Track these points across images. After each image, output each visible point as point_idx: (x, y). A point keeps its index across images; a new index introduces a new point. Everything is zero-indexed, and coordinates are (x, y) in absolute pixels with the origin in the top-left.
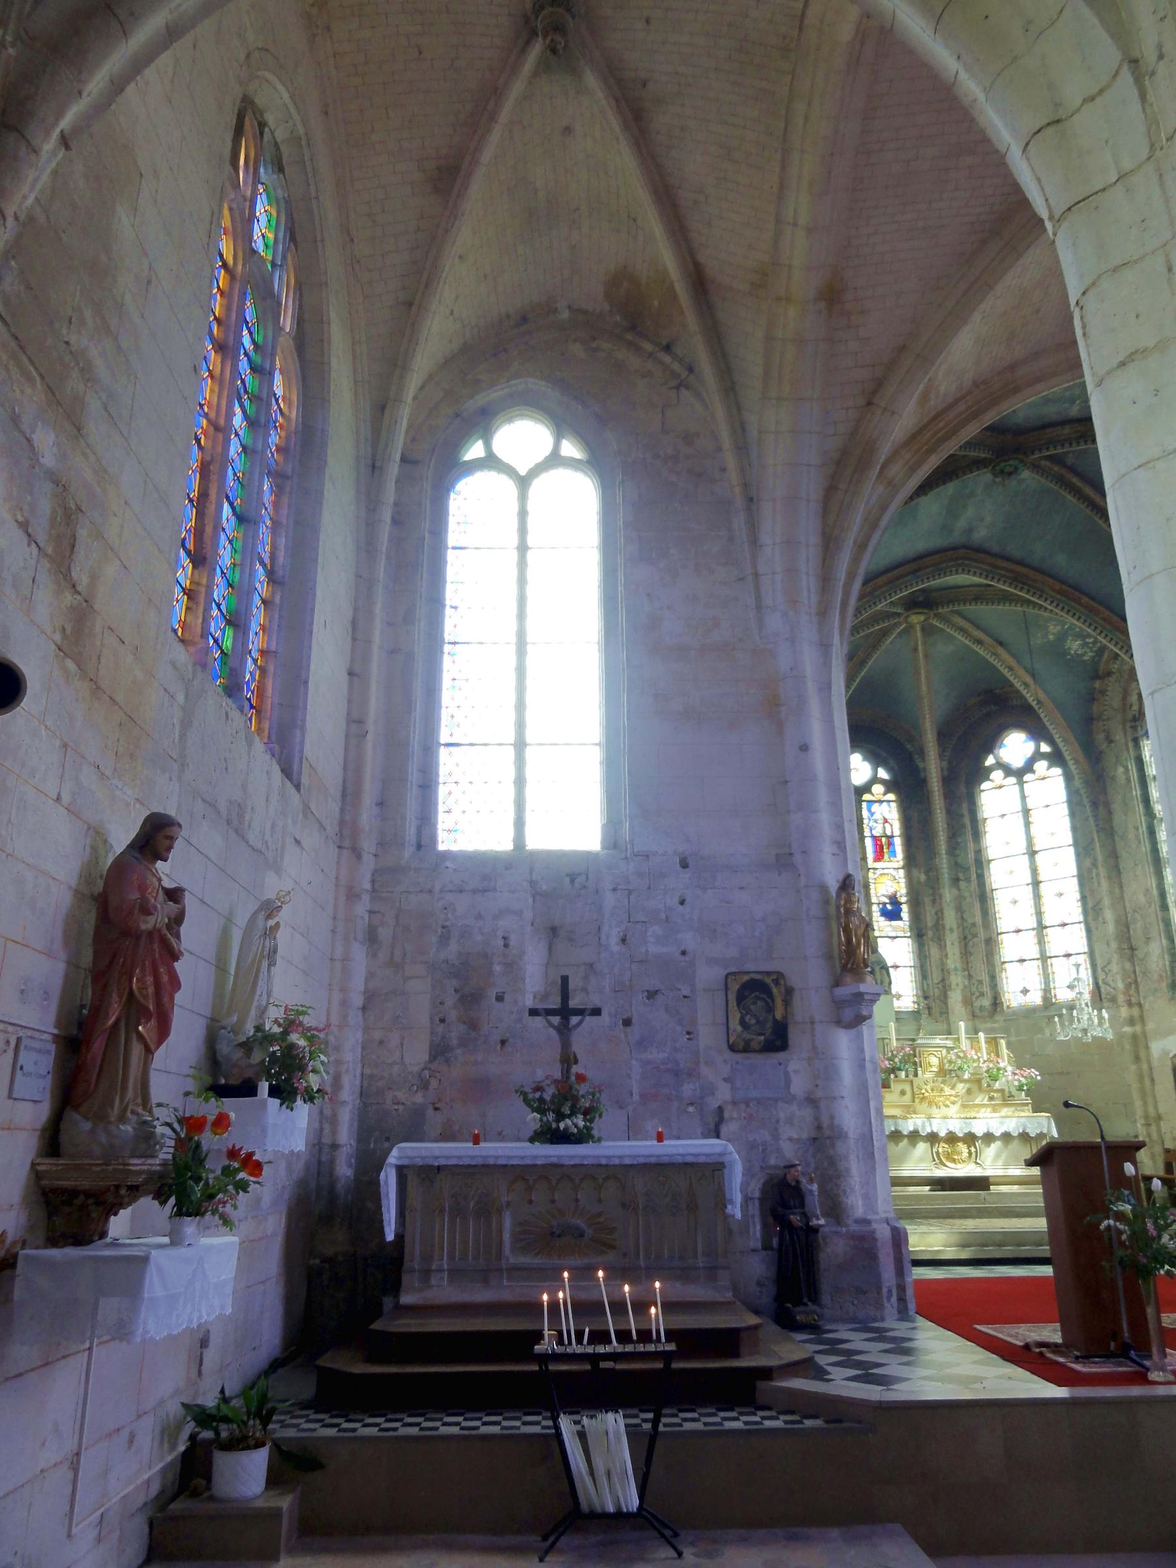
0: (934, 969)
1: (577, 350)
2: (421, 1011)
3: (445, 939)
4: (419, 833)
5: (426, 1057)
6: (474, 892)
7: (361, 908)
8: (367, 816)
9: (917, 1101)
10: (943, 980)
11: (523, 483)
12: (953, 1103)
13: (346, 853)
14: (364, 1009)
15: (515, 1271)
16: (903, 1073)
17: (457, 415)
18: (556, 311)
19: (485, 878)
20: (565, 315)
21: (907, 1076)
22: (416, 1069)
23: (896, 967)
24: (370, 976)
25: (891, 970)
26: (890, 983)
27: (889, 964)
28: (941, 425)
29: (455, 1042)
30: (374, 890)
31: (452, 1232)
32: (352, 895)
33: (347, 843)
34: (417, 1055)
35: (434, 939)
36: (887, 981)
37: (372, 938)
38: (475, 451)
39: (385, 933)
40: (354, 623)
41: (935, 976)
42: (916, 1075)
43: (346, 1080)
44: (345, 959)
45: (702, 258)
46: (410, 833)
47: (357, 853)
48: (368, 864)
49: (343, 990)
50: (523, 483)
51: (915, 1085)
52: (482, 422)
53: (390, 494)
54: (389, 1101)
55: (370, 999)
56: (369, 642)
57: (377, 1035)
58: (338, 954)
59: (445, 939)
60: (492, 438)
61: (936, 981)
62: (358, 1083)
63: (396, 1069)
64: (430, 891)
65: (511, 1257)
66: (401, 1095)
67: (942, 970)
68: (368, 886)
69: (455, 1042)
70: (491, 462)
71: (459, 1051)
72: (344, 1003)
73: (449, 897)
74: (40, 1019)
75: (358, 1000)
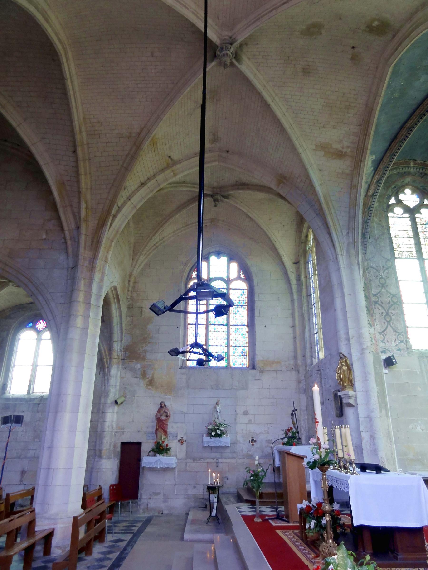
13: (297, 372)
28: (360, 149)
32: (299, 382)
62: (307, 429)
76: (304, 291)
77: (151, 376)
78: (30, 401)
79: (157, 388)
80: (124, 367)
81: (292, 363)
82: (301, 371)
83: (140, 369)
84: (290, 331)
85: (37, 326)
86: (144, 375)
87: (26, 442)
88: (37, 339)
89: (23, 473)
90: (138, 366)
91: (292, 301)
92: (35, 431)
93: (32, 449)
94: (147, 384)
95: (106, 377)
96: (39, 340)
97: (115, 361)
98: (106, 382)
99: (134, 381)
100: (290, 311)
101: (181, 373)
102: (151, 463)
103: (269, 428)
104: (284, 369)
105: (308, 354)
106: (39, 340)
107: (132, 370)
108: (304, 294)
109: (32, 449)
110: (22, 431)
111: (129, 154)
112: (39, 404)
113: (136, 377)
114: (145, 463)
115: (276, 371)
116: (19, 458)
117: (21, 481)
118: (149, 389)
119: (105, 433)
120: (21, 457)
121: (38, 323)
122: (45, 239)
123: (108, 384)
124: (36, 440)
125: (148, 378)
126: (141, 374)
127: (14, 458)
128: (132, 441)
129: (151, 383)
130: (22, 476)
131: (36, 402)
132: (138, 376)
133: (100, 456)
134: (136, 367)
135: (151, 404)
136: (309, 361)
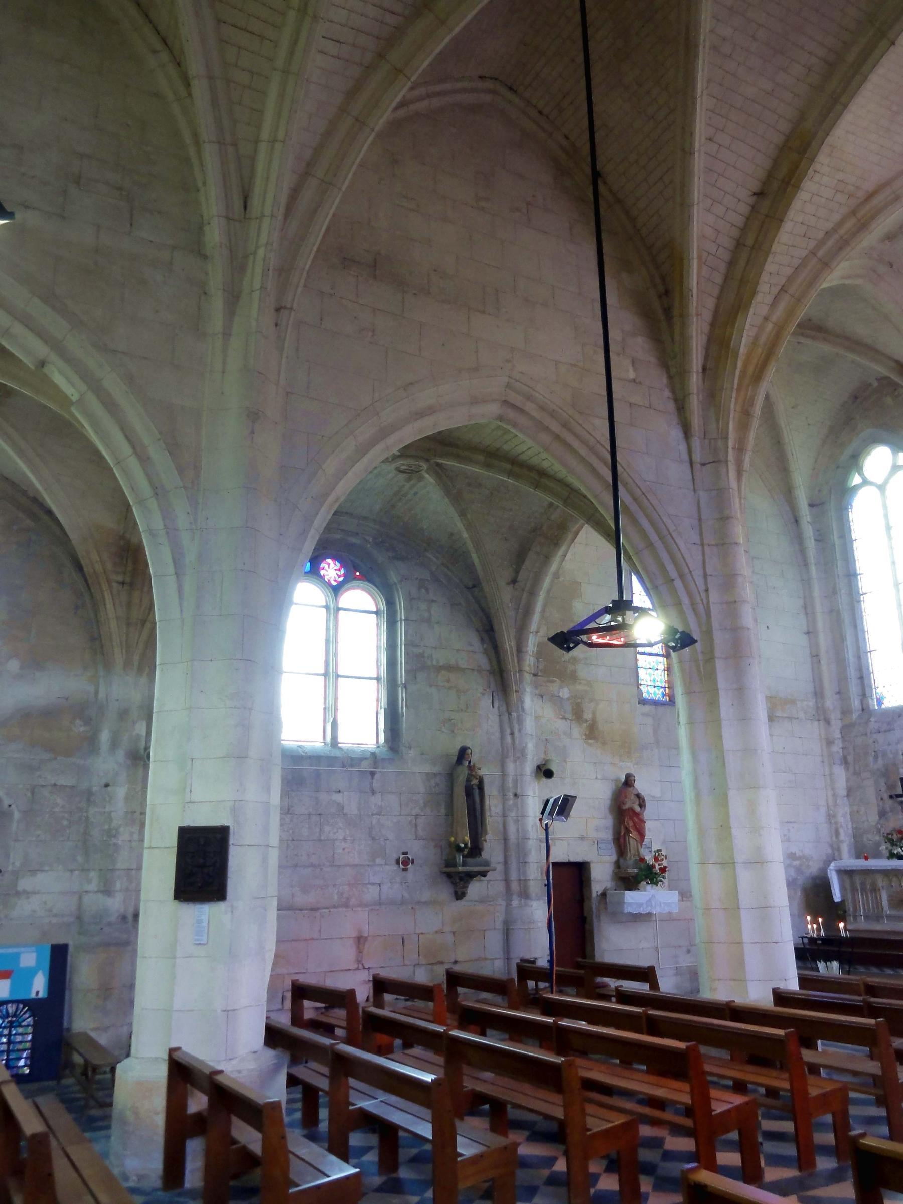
1: (889, 401)
2: (870, 793)
3: (876, 757)
4: (862, 704)
5: (877, 817)
6: (885, 732)
7: (837, 748)
8: (830, 701)
11: (882, 488)
13: (822, 723)
14: (848, 796)
15: (889, 917)
17: (838, 467)
18: (870, 385)
19: (889, 724)
20: (876, 384)
22: (874, 824)
24: (848, 780)
29: (888, 809)
30: (842, 737)
31: (863, 898)
32: (830, 743)
33: (822, 718)
34: (873, 818)
35: (871, 759)
37: (845, 761)
38: (856, 479)
39: (850, 758)
40: (805, 607)
43: (841, 831)
44: (831, 774)
45: (896, 357)
46: (856, 704)
47: (828, 722)
48: (836, 726)
49: (833, 789)
50: (882, 488)
52: (854, 462)
53: (809, 532)
54: (865, 839)
55: (850, 792)
56: (814, 613)
57: (855, 808)
58: (827, 773)
59: (876, 757)
60: (862, 468)
62: (850, 831)
63: (866, 823)
64: (866, 735)
65: (887, 910)
66: (870, 836)
68: (839, 736)
69: (888, 809)
70: (865, 482)
71: (890, 814)
72: (834, 795)
73: (875, 736)
74: (608, 835)
75: (842, 792)
76: (840, 564)
77: (590, 716)
78: (352, 765)
79: (604, 744)
80: (537, 692)
81: (811, 703)
82: (833, 722)
83: (568, 699)
84: (803, 640)
85: (322, 573)
86: (578, 715)
87: (356, 866)
88: (327, 607)
89: (360, 940)
90: (565, 693)
91: (806, 583)
92: (373, 839)
93: (373, 884)
94: (586, 735)
95: (514, 714)
96: (333, 611)
97: (528, 677)
98: (516, 727)
99: (561, 725)
100: (801, 602)
101: (643, 715)
102: (641, 905)
103: (789, 830)
104: (801, 715)
105: (854, 689)
106: (333, 611)
107: (555, 700)
108: (840, 570)
109: (373, 884)
110: (345, 840)
111: (835, 230)
112: (373, 774)
113: (564, 718)
114: (629, 904)
115: (790, 718)
116: (346, 905)
117: (359, 961)
118: (591, 745)
119: (530, 842)
120: (351, 903)
121: (322, 565)
122: (634, 381)
123: (520, 731)
124: (379, 861)
125: (587, 721)
126: (573, 709)
127: (334, 907)
128: (572, 860)
129: (592, 733)
130: (360, 951)
131: (365, 766)
132: (569, 716)
133: (525, 895)
134: (561, 694)
135: (597, 778)
136: (856, 704)
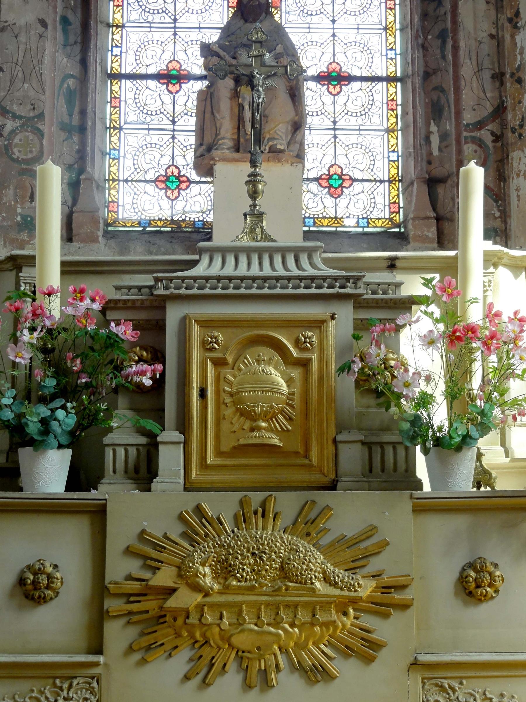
0: (467, 70)
9: (118, 635)
10: (500, 111)
12: (367, 649)
16: (50, 471)
21: (81, 477)
23: (334, 78)
25: (314, 95)
26: (298, 126)
27: (312, 62)
36: (280, 112)
41: (468, 97)
42: (144, 472)
51: (121, 533)
61: (468, 117)
67: (499, 77)
